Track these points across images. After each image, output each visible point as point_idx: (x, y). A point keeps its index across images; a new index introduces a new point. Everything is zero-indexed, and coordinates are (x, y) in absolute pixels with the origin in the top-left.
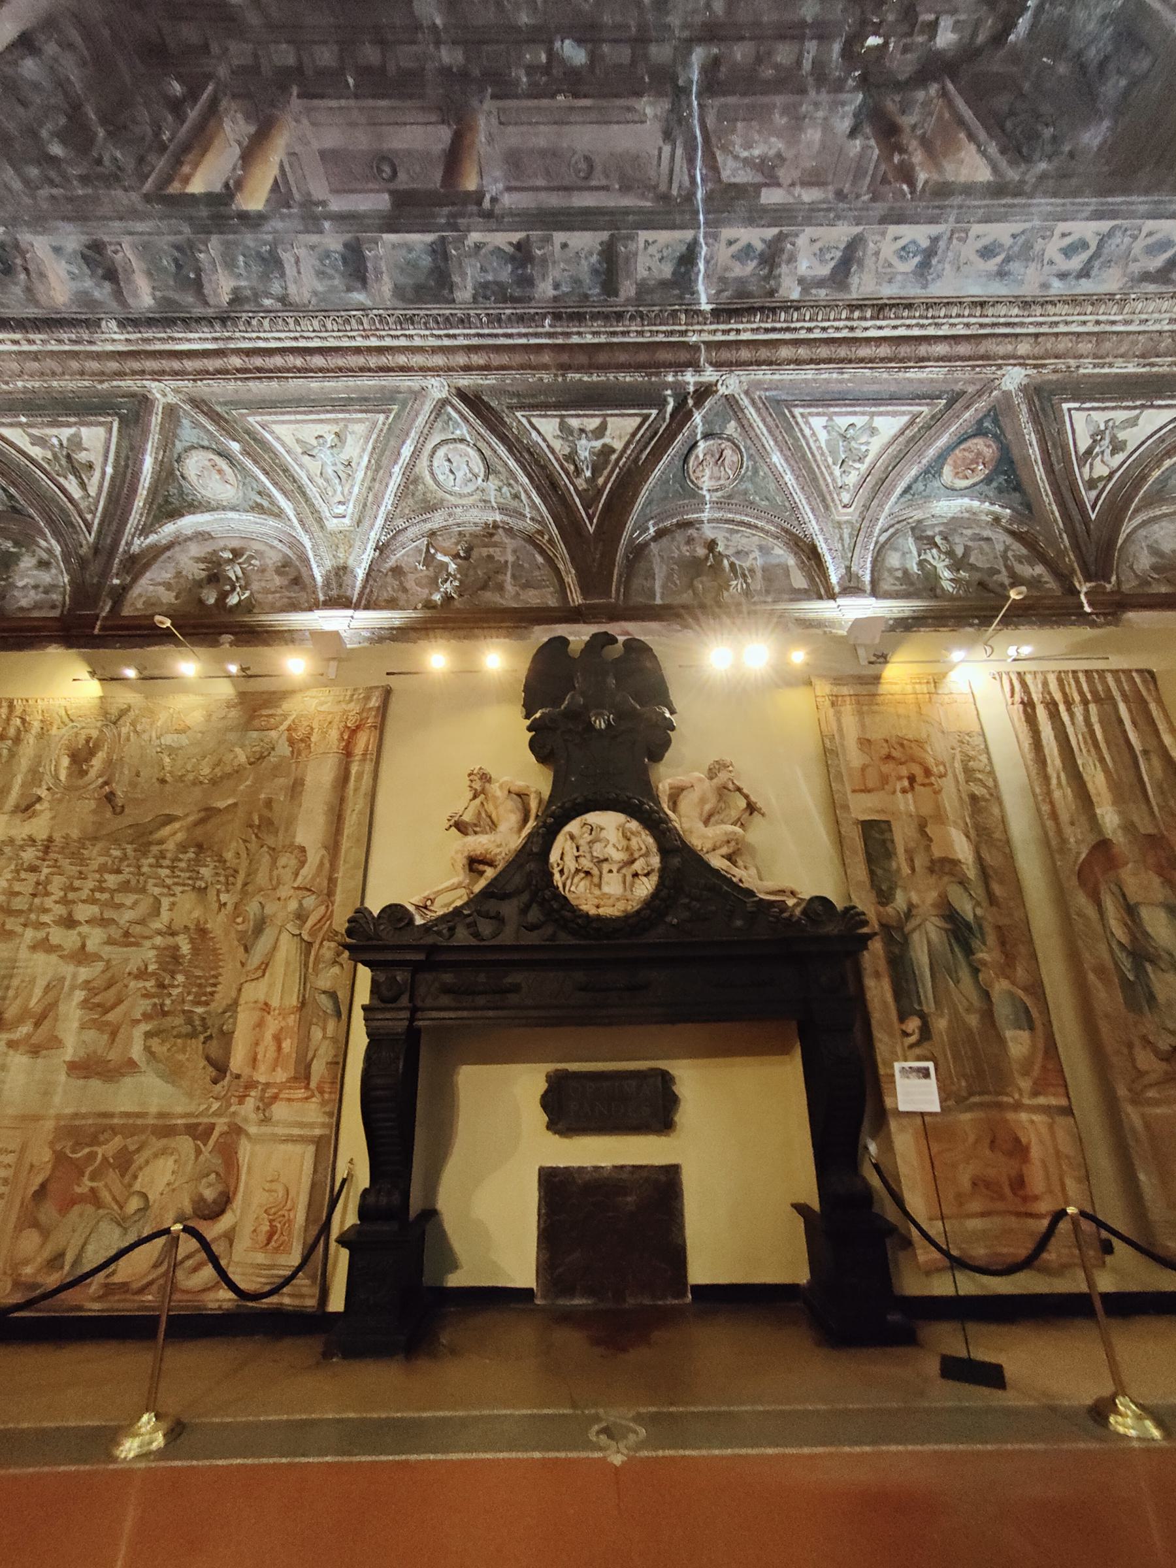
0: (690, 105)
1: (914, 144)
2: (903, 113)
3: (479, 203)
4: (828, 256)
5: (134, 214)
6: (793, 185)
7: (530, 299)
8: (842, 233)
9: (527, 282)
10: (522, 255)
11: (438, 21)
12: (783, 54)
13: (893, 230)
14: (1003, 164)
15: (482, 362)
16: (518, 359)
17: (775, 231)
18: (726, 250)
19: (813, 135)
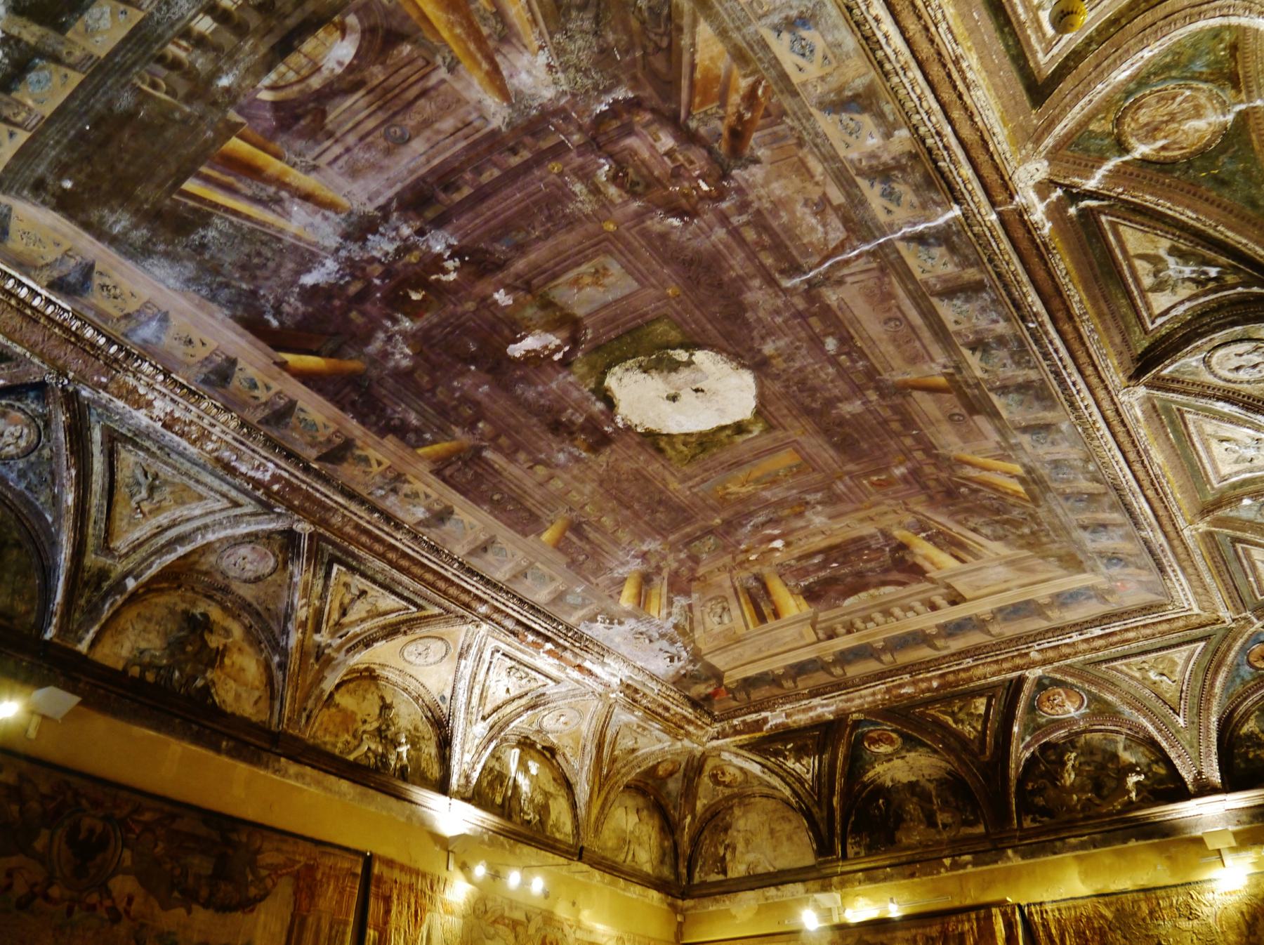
0: (815, 277)
1: (731, 109)
2: (720, 135)
3: (952, 374)
4: (852, 124)
5: (1050, 511)
6: (817, 184)
7: (1015, 335)
8: (826, 123)
9: (1001, 341)
10: (980, 345)
11: (859, 402)
12: (750, 235)
13: (796, 78)
14: (686, 21)
15: (1091, 368)
16: (1076, 346)
17: (859, 180)
18: (899, 215)
19: (778, 189)
